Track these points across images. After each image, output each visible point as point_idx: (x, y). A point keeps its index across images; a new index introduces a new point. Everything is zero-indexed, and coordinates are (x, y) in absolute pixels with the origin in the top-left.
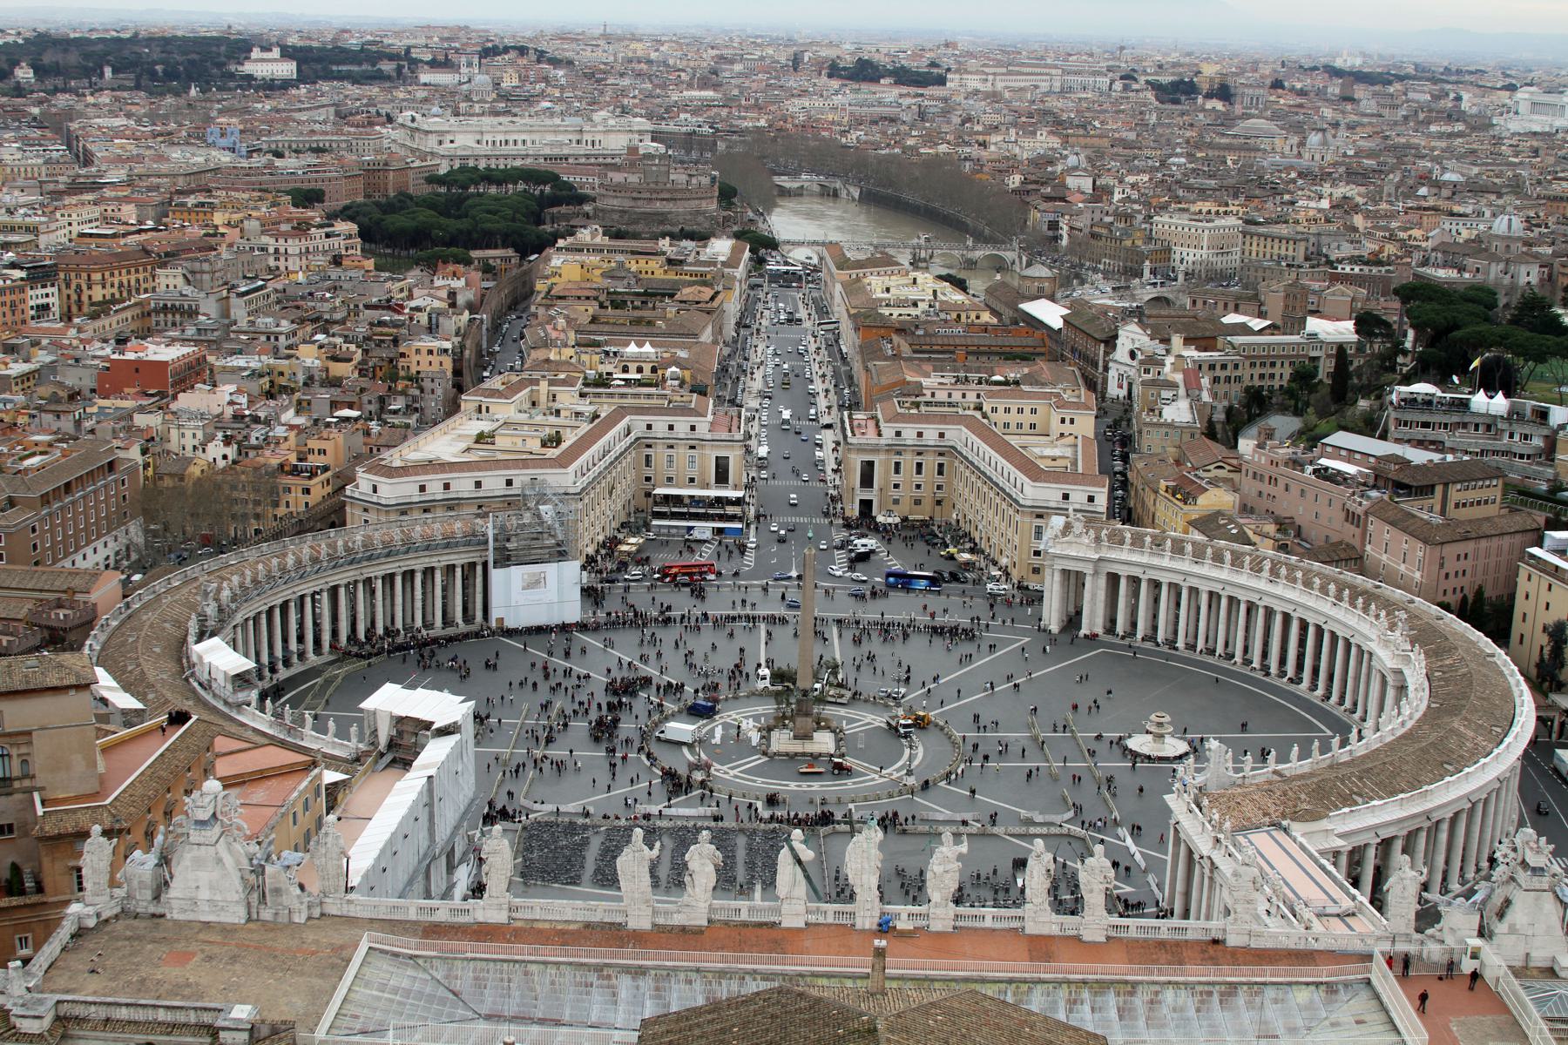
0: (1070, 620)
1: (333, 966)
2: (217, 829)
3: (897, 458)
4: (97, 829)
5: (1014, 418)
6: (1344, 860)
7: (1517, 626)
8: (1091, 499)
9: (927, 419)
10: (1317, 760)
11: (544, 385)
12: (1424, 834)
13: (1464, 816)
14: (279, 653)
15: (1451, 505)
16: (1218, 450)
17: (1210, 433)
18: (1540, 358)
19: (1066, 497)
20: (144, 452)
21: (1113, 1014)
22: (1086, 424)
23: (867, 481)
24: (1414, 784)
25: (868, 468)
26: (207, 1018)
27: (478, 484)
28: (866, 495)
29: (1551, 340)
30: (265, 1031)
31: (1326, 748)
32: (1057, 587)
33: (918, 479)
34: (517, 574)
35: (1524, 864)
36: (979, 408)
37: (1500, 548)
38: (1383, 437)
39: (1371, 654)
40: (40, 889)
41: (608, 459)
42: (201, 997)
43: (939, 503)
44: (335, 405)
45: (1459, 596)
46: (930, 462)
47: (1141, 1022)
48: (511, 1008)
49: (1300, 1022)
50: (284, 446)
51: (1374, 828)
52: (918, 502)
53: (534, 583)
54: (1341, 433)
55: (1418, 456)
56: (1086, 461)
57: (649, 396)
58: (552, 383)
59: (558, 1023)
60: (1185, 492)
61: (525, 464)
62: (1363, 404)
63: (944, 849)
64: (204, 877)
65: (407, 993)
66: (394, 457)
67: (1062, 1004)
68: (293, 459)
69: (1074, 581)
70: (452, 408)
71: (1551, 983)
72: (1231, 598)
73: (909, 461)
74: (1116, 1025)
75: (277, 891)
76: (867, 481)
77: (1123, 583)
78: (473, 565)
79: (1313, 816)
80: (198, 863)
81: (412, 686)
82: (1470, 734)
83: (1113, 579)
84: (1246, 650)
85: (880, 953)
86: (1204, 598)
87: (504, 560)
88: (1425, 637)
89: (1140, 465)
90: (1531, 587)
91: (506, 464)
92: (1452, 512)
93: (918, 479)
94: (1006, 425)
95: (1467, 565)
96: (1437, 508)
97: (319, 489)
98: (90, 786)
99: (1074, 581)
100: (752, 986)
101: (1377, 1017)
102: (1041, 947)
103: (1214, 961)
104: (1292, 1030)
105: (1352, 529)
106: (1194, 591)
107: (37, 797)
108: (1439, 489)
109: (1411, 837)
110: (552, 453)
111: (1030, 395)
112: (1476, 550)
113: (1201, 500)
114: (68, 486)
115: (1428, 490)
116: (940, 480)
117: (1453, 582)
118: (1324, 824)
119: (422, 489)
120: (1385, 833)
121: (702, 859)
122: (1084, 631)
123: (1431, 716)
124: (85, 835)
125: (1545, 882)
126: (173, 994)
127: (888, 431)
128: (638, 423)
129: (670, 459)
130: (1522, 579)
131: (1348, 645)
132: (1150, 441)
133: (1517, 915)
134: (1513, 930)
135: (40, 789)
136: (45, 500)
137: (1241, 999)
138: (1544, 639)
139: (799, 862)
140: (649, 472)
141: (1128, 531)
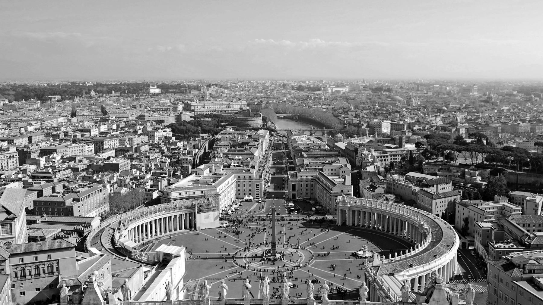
0: (33, 239)
3: (301, 183)
5: (330, 172)
8: (349, 191)
10: (403, 256)
14: (141, 237)
15: (439, 189)
16: (381, 178)
18: (460, 151)
19: (342, 191)
23: (294, 189)
24: (427, 261)
25: (294, 186)
27: (194, 193)
28: (294, 193)
29: (462, 147)
32: (340, 214)
33: (307, 188)
34: (203, 215)
36: (321, 170)
38: (422, 173)
41: (228, 186)
43: (312, 194)
44: (162, 174)
45: (441, 212)
46: (309, 183)
50: (147, 184)
51: (417, 274)
52: (307, 194)
53: (207, 217)
54: (411, 172)
55: (430, 177)
57: (239, 169)
58: (215, 167)
60: (373, 188)
61: (206, 188)
66: (173, 187)
68: (149, 187)
69: (343, 212)
70: (191, 174)
73: (304, 184)
76: (294, 189)
77: (356, 212)
79: (401, 271)
81: (169, 245)
82: (442, 248)
83: (354, 212)
84: (388, 228)
87: (200, 212)
91: (201, 187)
92: (439, 191)
93: (307, 188)
94: (329, 174)
95: (442, 204)
96: (435, 190)
97: (155, 195)
99: (343, 212)
107: (60, 277)
108: (435, 186)
112: (445, 201)
113: (376, 190)
115: (433, 186)
116: (312, 188)
117: (440, 209)
118: (402, 273)
119: (180, 194)
120: (420, 275)
123: (433, 244)
129: (244, 185)
130: (457, 207)
131: (412, 226)
135: (61, 275)
138: (463, 222)
140: (239, 188)
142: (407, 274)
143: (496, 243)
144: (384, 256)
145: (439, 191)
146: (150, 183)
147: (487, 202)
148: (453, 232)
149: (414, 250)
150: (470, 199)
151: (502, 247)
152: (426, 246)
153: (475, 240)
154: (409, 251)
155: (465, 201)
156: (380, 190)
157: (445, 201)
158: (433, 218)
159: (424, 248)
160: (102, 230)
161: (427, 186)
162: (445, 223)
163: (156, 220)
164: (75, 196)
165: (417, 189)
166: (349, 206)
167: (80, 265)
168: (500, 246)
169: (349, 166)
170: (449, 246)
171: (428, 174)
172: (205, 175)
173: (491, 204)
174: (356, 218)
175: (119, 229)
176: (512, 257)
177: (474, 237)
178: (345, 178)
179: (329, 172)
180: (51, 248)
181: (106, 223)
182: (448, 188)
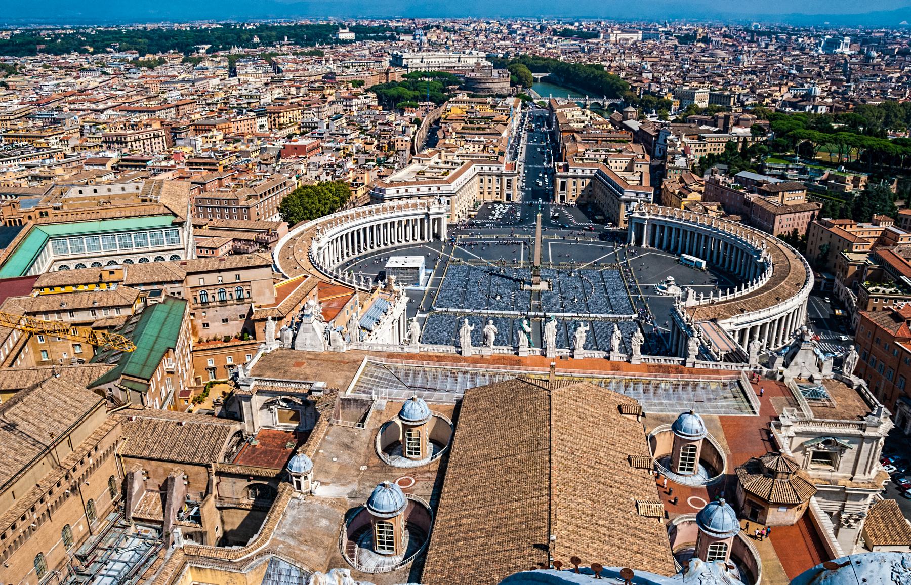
1: (354, 368)
2: (313, 318)
4: (270, 318)
5: (619, 165)
6: (737, 334)
7: (809, 247)
9: (586, 165)
10: (729, 297)
11: (443, 153)
12: (768, 325)
13: (784, 319)
15: (786, 199)
16: (697, 177)
17: (694, 171)
18: (823, 142)
20: (297, 178)
21: (641, 391)
22: (645, 169)
23: (563, 187)
24: (765, 306)
25: (563, 184)
26: (308, 387)
30: (328, 391)
31: (732, 292)
35: (802, 340)
36: (605, 161)
37: (803, 218)
38: (762, 172)
39: (752, 256)
40: (255, 338)
42: (306, 379)
43: (590, 197)
46: (588, 181)
47: (652, 395)
48: (418, 384)
49: (711, 396)
55: (772, 180)
56: (646, 182)
59: (435, 390)
61: (436, 183)
62: (752, 160)
63: (580, 329)
64: (308, 335)
65: (381, 378)
66: (387, 180)
67: (622, 388)
68: (351, 181)
70: (411, 162)
71: (811, 384)
72: (699, 234)
74: (642, 396)
75: (335, 340)
76: (563, 189)
77: (658, 228)
78: (416, 220)
80: (306, 330)
83: (654, 226)
85: (552, 367)
86: (689, 233)
88: (774, 249)
89: (666, 183)
90: (815, 232)
92: (785, 203)
98: (273, 301)
100: (507, 378)
101: (742, 395)
102: (616, 367)
103: (681, 372)
104: (709, 400)
105: (746, 208)
106: (685, 232)
108: (781, 194)
109: (763, 326)
110: (446, 178)
111: (625, 156)
114: (269, 191)
115: (776, 194)
116: (590, 188)
117: (783, 230)
118: (729, 320)
120: (753, 324)
121: (491, 330)
122: (644, 246)
123: (774, 281)
124: (266, 319)
125: (810, 347)
126: (296, 377)
127: (571, 170)
128: (477, 168)
131: (743, 252)
132: (670, 173)
133: (798, 358)
134: (796, 364)
136: (261, 196)
137: (690, 388)
139: (525, 332)
140: (482, 185)
141: (660, 208)
142: (736, 321)
143: (873, 285)
144: (702, 295)
145: (785, 203)
146: (351, 175)
147: (860, 224)
148: (805, 264)
149: (746, 287)
150: (834, 218)
151: (880, 292)
152: (765, 283)
153: (837, 281)
154: (739, 290)
155: (826, 219)
156: (695, 197)
157: (803, 218)
158: (775, 242)
159: (761, 286)
160: (293, 240)
161: (768, 194)
162: (794, 252)
163: (365, 229)
164: (248, 191)
165: (753, 197)
166: (647, 217)
167: (278, 289)
168: (877, 290)
169: (647, 157)
170: (799, 286)
171: (769, 175)
172: (432, 163)
173: (867, 226)
174: (657, 236)
175: (318, 241)
176: (899, 308)
177: (834, 274)
178: (641, 176)
179: (616, 165)
180: (239, 266)
181: (296, 231)
182: (799, 198)
